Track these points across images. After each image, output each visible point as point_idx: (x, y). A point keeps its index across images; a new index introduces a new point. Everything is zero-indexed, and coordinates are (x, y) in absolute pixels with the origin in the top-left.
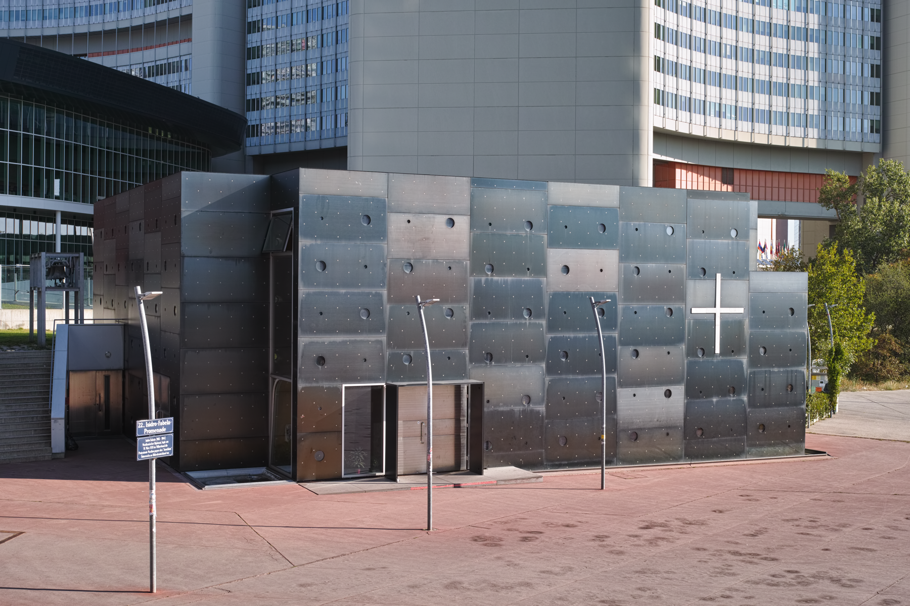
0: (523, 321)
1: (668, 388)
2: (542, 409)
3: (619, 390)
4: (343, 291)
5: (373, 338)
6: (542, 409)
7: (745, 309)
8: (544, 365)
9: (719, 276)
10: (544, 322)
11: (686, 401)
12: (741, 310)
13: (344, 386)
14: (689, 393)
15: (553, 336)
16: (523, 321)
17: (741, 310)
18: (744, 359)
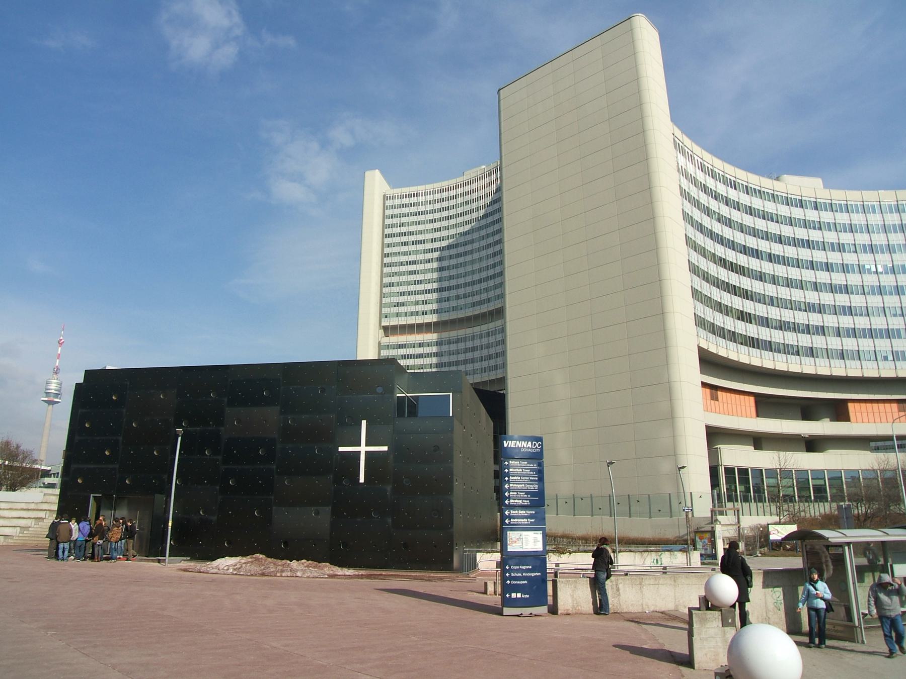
0: (206, 457)
1: (315, 508)
2: (214, 518)
3: (274, 508)
4: (98, 438)
5: (111, 466)
6: (214, 518)
7: (388, 448)
8: (218, 487)
9: (364, 423)
10: (220, 458)
11: (332, 520)
12: (385, 448)
13: (92, 495)
14: (334, 512)
15: (226, 467)
16: (206, 457)
17: (385, 448)
18: (389, 488)
